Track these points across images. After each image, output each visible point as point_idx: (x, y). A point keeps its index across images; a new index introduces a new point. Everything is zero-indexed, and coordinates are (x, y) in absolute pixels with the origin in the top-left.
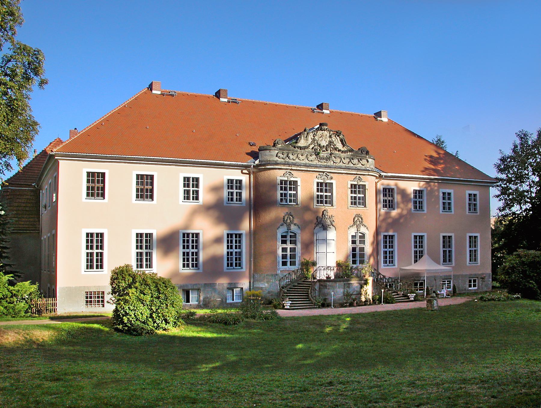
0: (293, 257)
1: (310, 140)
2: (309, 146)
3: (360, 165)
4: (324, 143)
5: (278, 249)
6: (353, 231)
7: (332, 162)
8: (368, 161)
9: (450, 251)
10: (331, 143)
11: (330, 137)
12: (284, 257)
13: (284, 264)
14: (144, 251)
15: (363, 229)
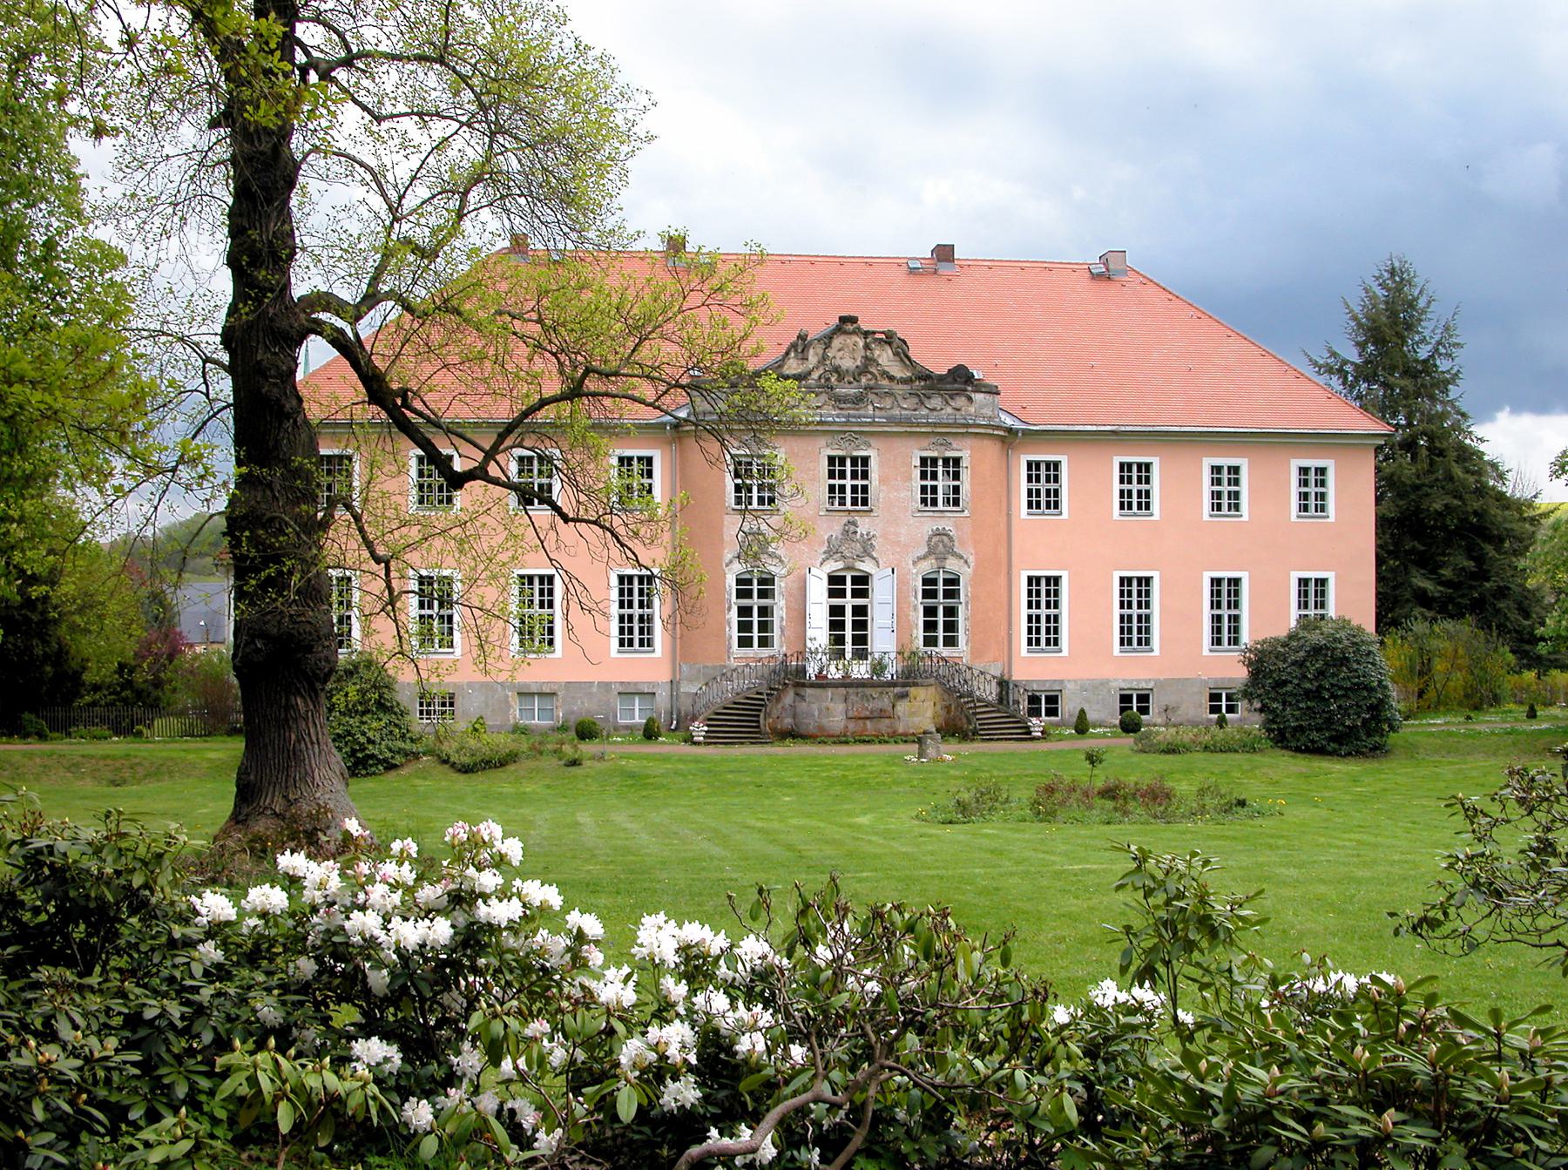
0: (764, 627)
1: (813, 359)
2: (809, 373)
3: (949, 410)
4: (847, 363)
5: (729, 609)
6: (927, 567)
7: (870, 407)
8: (970, 399)
9: (1235, 619)
10: (869, 360)
11: (867, 347)
12: (744, 627)
13: (745, 642)
14: (636, 611)
15: (952, 565)
